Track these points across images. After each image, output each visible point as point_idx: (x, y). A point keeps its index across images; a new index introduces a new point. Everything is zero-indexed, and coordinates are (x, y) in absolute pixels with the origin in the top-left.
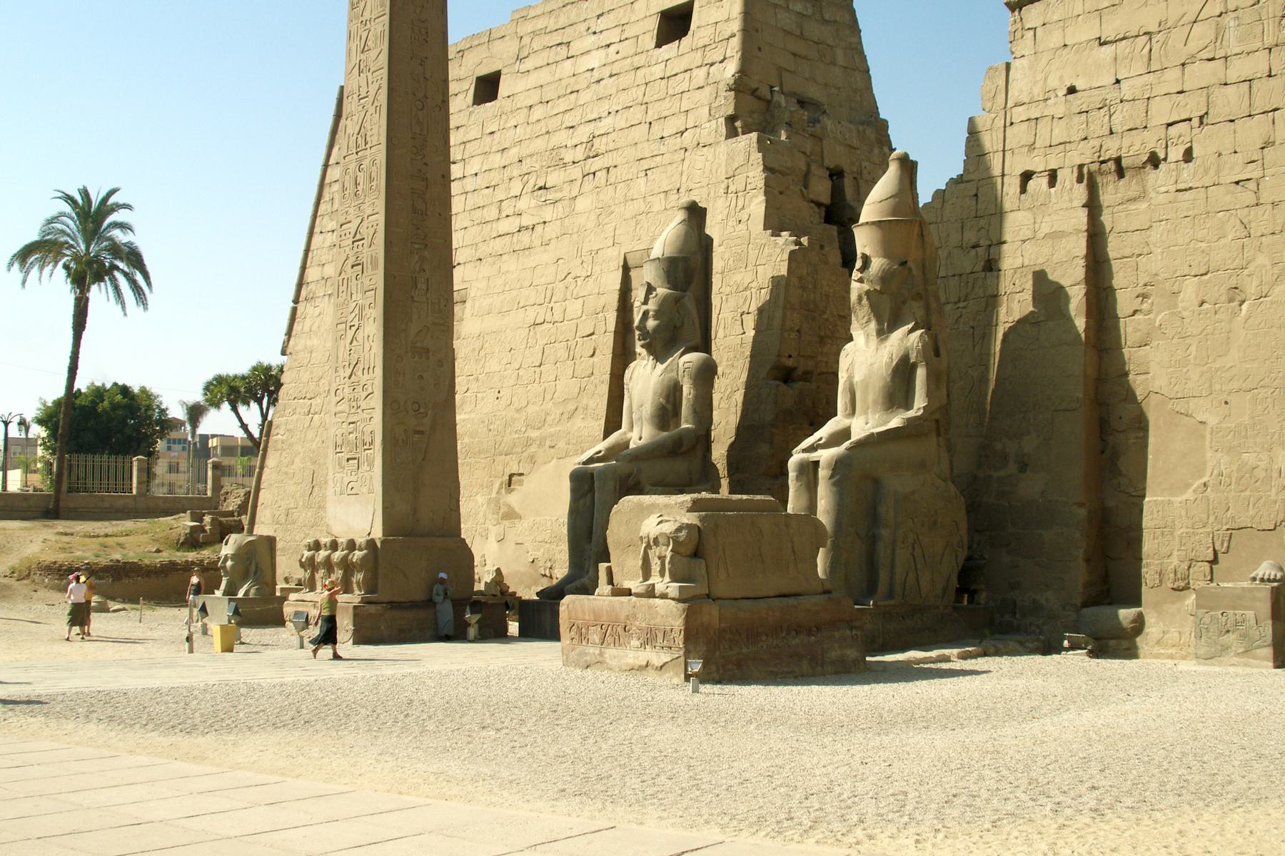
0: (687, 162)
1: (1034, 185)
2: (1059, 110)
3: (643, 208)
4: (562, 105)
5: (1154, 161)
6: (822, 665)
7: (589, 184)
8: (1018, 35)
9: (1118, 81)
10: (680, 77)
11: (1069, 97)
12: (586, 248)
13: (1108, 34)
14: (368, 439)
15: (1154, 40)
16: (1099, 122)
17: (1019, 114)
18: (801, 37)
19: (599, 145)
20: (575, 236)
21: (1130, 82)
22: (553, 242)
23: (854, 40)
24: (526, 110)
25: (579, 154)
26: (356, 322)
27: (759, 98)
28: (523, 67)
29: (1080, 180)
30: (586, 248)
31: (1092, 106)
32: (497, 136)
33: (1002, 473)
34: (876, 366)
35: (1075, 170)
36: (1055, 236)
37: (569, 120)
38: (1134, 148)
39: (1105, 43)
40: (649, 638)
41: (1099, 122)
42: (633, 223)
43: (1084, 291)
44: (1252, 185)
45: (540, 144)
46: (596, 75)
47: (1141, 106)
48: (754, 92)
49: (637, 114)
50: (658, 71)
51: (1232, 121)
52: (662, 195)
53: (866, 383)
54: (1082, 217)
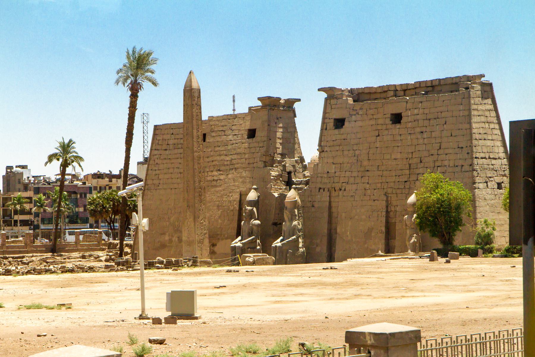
1: (322, 190)
5: (340, 190)
54: (328, 199)
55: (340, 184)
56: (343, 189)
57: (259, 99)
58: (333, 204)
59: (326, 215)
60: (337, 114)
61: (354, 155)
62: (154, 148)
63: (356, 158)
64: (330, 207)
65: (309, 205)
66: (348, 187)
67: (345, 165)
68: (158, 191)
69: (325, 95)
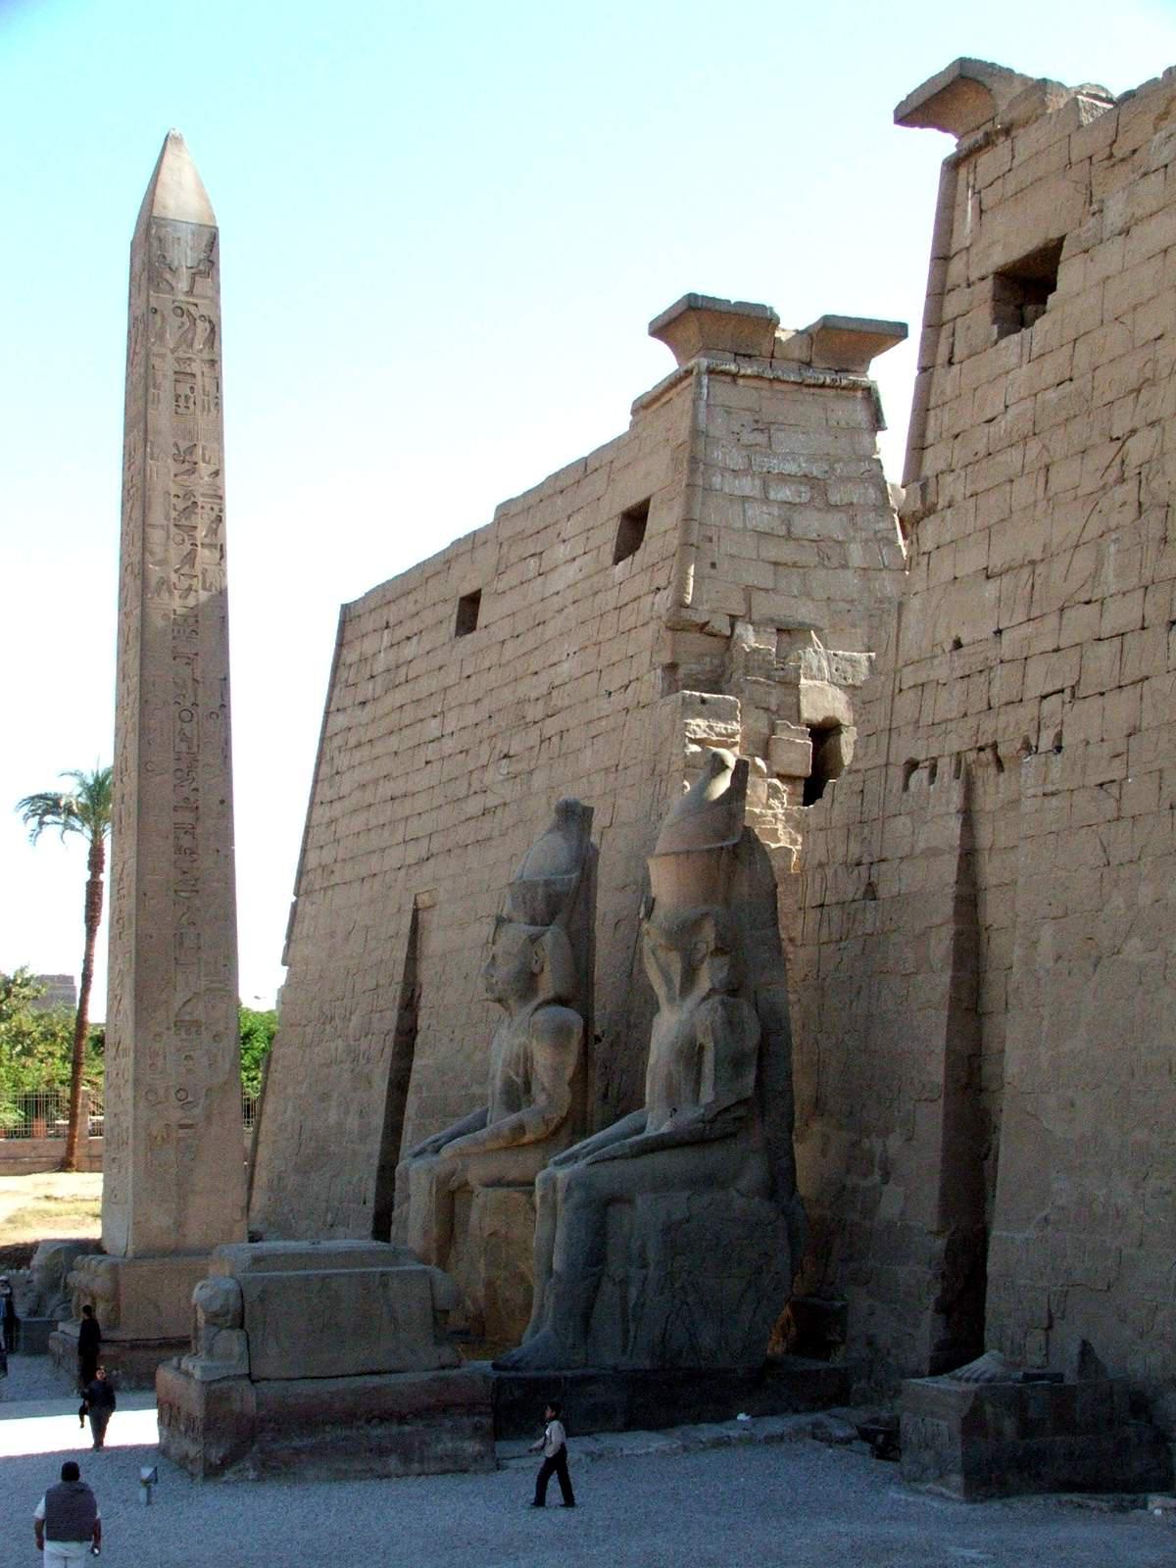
1: (920, 776)
2: (941, 672)
4: (530, 641)
5: (1028, 747)
6: (421, 1461)
10: (630, 607)
13: (997, 563)
15: (1037, 572)
18: (789, 536)
19: (558, 699)
22: (510, 831)
24: (498, 646)
27: (712, 635)
28: (501, 586)
32: (473, 678)
33: (864, 1183)
35: (954, 758)
36: (933, 853)
37: (535, 663)
38: (1008, 727)
44: (1114, 790)
45: (507, 696)
50: (610, 599)
51: (1102, 694)
54: (955, 825)
55: (1028, 711)
56: (1046, 741)
57: (663, 329)
58: (990, 871)
59: (941, 945)
60: (1010, 241)
61: (1114, 473)
62: (333, 708)
63: (1127, 492)
64: (969, 899)
65: (851, 888)
66: (1083, 723)
67: (1058, 568)
68: (330, 892)
69: (941, 144)
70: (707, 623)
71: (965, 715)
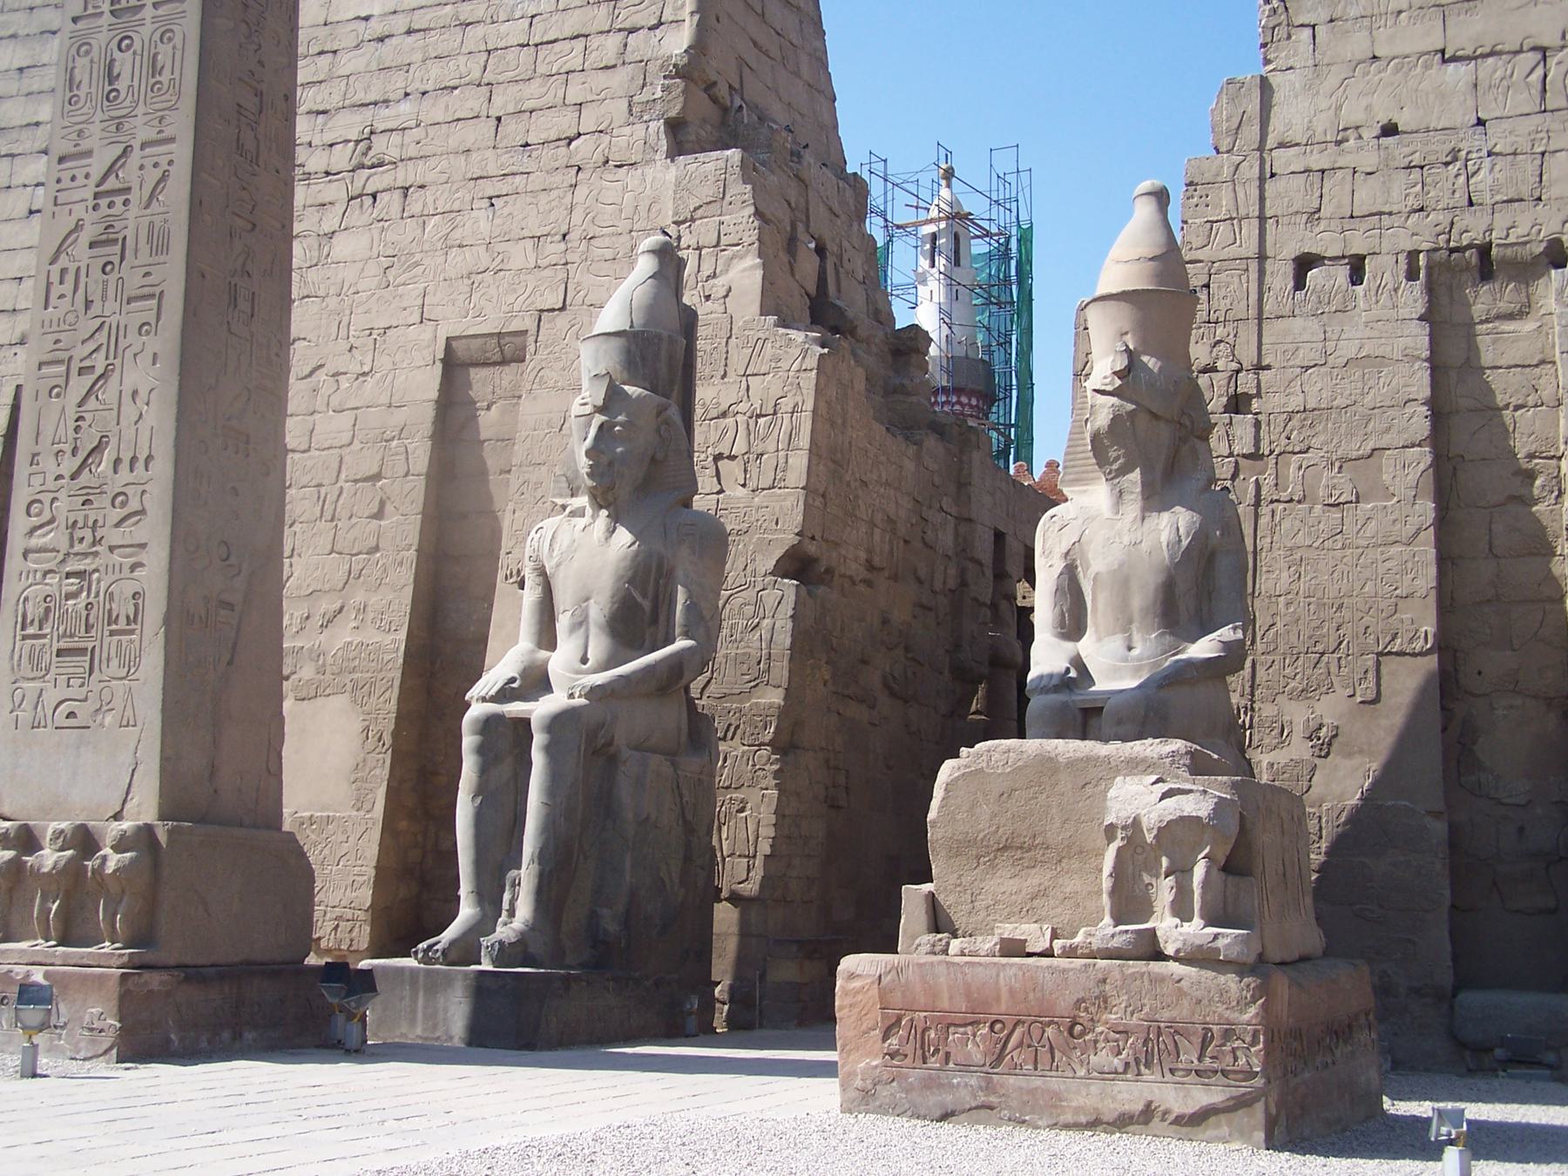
0: (581, 191)
2: (1368, 160)
3: (485, 261)
7: (356, 217)
8: (1281, 32)
9: (1481, 122)
11: (1385, 141)
12: (359, 321)
14: (124, 608)
15: (1552, 62)
16: (1445, 186)
17: (1282, 160)
20: (332, 302)
21: (1506, 125)
23: (818, 44)
25: (341, 158)
26: (100, 362)
29: (1412, 275)
30: (359, 321)
31: (1432, 158)
34: (1144, 546)
35: (1402, 258)
39: (1454, 59)
40: (1152, 1049)
41: (1445, 186)
42: (464, 286)
43: (1428, 459)
46: (375, 27)
47: (1530, 167)
48: (710, 87)
49: (471, 101)
52: (529, 243)
53: (1121, 581)
70: (715, 83)
71: (1422, 209)
